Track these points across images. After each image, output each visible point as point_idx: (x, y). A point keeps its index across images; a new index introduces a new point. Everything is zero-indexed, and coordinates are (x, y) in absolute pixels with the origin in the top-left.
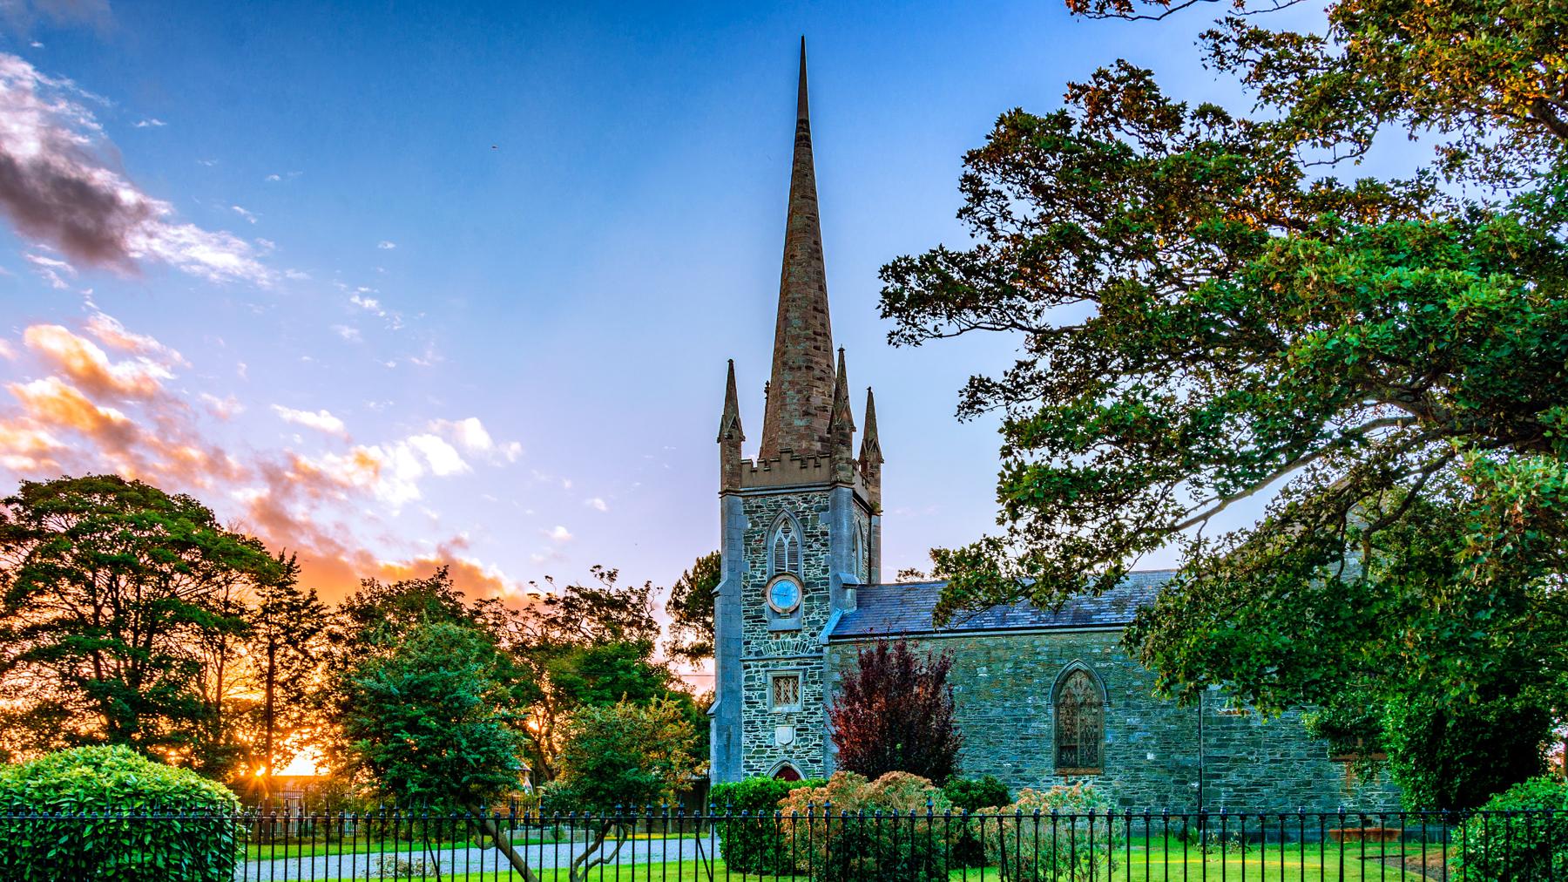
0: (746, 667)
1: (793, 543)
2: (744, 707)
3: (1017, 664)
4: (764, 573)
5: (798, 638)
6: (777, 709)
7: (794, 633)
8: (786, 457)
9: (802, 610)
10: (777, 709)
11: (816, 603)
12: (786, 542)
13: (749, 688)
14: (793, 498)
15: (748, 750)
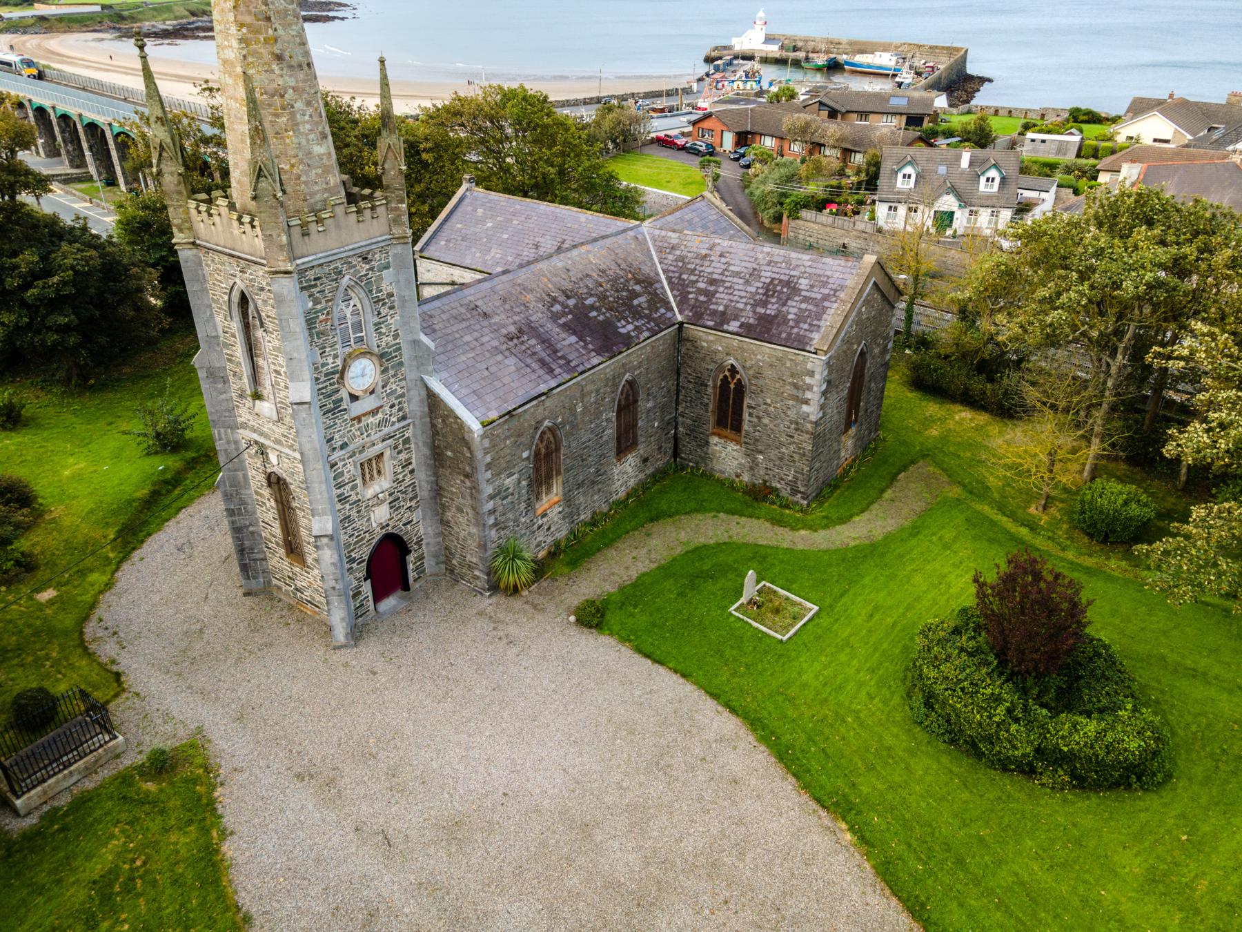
1: (356, 313)
2: (339, 506)
5: (380, 415)
6: (370, 492)
7: (374, 412)
9: (381, 384)
10: (370, 492)
12: (348, 312)
13: (339, 486)
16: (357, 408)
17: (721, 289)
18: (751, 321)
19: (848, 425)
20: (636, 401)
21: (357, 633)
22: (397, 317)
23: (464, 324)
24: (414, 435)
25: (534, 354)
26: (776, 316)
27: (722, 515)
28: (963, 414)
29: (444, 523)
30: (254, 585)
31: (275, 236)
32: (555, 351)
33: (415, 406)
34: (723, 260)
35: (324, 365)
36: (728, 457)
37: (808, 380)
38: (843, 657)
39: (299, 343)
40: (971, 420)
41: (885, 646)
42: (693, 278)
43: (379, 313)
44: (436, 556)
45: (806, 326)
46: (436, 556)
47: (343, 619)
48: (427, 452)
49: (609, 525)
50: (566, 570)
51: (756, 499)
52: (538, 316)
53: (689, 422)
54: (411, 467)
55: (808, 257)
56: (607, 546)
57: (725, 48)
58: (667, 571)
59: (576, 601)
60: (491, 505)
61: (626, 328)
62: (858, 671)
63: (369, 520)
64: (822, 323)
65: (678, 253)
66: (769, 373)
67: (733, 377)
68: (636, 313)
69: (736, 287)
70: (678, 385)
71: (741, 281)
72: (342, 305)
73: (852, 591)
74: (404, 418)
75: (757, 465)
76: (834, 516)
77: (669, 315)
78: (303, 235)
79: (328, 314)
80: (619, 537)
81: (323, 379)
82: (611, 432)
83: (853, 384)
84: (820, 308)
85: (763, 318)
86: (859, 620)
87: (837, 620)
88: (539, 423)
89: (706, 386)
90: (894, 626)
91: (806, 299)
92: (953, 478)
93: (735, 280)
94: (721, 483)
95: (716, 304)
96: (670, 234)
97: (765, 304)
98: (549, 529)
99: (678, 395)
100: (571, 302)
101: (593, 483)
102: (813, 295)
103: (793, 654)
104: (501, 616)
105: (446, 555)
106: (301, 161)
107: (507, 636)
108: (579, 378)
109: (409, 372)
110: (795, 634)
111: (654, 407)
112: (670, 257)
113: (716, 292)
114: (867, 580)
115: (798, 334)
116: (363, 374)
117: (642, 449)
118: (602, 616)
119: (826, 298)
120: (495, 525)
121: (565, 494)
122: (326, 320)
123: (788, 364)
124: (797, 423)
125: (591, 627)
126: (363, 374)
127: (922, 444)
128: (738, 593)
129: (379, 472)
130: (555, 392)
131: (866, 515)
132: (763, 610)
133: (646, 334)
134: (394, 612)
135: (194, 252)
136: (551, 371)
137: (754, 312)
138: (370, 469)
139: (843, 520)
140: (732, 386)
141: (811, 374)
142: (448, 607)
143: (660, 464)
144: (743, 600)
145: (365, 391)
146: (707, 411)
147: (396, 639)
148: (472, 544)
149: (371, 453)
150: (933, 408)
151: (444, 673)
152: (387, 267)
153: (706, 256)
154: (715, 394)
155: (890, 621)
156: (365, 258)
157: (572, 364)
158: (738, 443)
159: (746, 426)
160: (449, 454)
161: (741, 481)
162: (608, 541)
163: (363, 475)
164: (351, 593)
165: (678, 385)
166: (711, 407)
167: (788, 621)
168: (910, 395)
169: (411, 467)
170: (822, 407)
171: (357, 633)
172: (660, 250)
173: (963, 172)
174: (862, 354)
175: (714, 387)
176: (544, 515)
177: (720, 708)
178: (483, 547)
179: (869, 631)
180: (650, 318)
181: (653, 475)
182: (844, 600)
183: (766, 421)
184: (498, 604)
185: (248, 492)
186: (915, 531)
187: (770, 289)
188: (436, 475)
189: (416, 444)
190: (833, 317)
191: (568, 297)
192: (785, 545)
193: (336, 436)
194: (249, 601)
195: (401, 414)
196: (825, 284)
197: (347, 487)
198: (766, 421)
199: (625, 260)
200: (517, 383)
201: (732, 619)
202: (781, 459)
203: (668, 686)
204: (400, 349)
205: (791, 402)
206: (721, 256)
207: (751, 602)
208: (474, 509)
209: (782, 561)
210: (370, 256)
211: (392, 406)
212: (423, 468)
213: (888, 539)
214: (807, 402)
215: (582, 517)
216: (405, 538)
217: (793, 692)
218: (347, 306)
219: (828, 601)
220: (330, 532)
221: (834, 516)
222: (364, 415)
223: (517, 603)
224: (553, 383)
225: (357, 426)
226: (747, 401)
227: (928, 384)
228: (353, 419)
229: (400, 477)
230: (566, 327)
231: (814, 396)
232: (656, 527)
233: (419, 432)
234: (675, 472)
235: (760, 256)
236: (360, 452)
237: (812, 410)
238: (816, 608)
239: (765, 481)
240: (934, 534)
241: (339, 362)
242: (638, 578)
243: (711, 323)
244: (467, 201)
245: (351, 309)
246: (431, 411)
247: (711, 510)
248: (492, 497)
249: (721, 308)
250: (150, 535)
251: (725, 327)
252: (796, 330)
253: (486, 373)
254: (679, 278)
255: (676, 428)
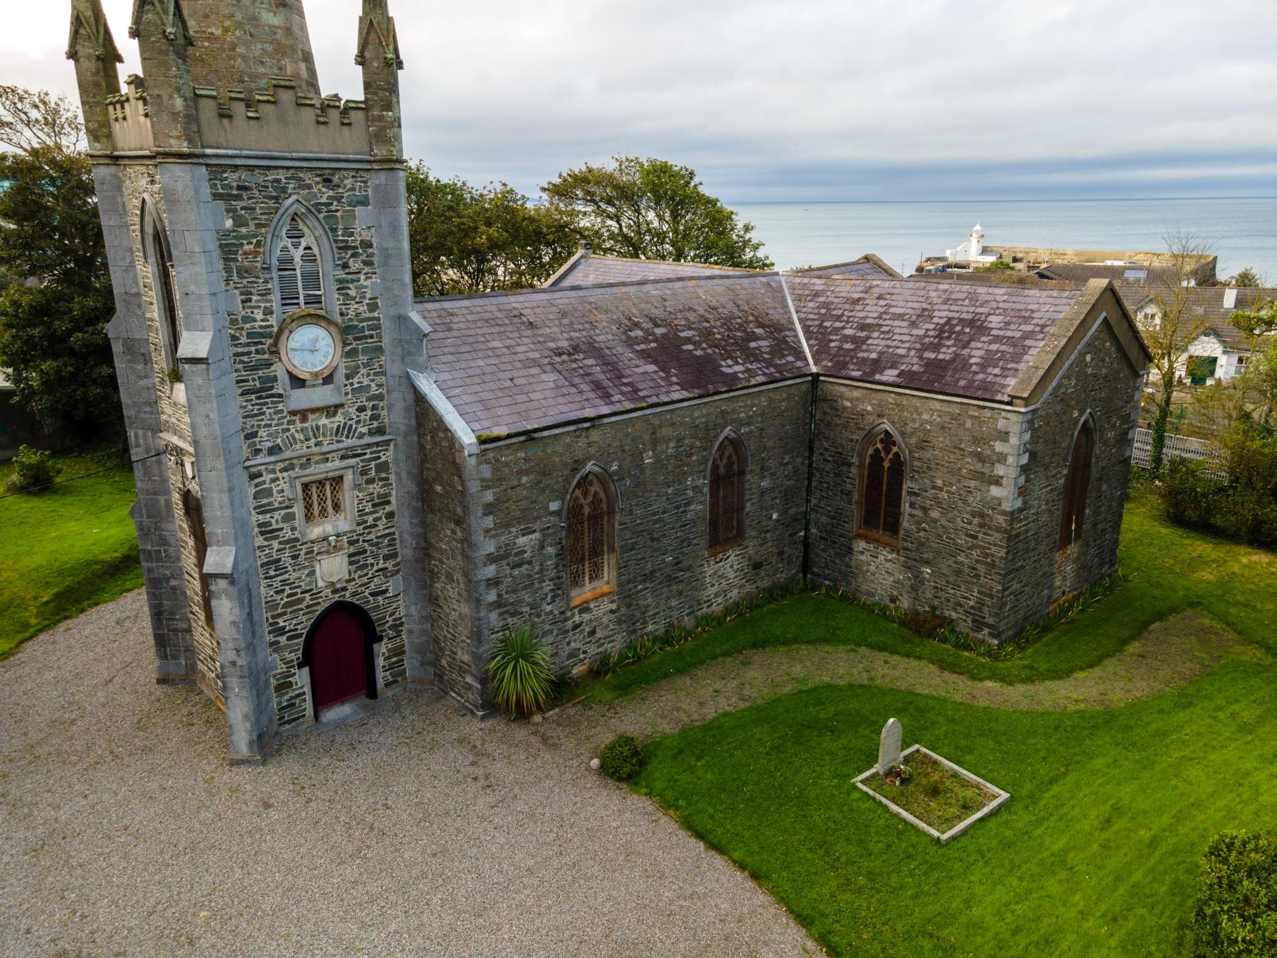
0: (253, 477)
1: (309, 257)
2: (260, 541)
3: (679, 440)
4: (268, 312)
5: (339, 418)
6: (316, 531)
7: (331, 410)
8: (286, 97)
9: (342, 372)
10: (316, 531)
11: (363, 359)
12: (297, 255)
13: (262, 510)
14: (308, 178)
15: (272, 605)
16: (301, 399)
17: (876, 334)
18: (915, 368)
19: (1065, 541)
20: (742, 473)
21: (268, 744)
22: (376, 279)
23: (497, 329)
24: (396, 461)
25: (588, 374)
26: (952, 361)
27: (863, 650)
28: (1255, 558)
29: (433, 600)
30: (177, 668)
31: (165, 98)
32: (620, 377)
33: (396, 417)
34: (882, 302)
35: (247, 319)
36: (879, 569)
37: (999, 446)
38: (1053, 886)
39: (197, 269)
40: (1269, 564)
41: (1137, 877)
42: (838, 324)
43: (345, 266)
44: (420, 651)
45: (997, 371)
46: (420, 651)
47: (246, 716)
48: (413, 488)
49: (690, 644)
50: (609, 696)
51: (918, 633)
52: (606, 337)
53: (824, 519)
54: (388, 509)
55: (1004, 291)
56: (679, 672)
57: (939, 259)
58: (761, 714)
59: (608, 738)
60: (491, 570)
61: (730, 367)
62: (1083, 915)
63: (312, 573)
64: (1022, 366)
65: (822, 299)
66: (940, 440)
67: (888, 451)
68: (752, 356)
69: (897, 330)
70: (810, 465)
71: (905, 324)
72: (288, 243)
73: (1071, 778)
74: (380, 431)
75: (922, 582)
76: (1043, 667)
77: (799, 364)
78: (222, 116)
79: (258, 244)
80: (702, 662)
81: (243, 340)
82: (699, 507)
83: (1071, 479)
84: (1019, 348)
85: (930, 364)
86: (1086, 825)
87: (1041, 821)
88: (578, 463)
89: (849, 465)
90: (1153, 843)
91: (997, 339)
92: (1245, 636)
93: (896, 323)
94: (869, 609)
95: (867, 351)
96: (814, 281)
97: (936, 348)
98: (592, 633)
99: (810, 480)
100: (659, 331)
101: (670, 579)
102: (1009, 334)
103: (958, 867)
104: (489, 747)
105: (433, 650)
106: (239, 25)
107: (487, 777)
108: (648, 412)
109: (392, 365)
110: (964, 832)
111: (772, 490)
112: (811, 305)
113: (868, 338)
114: (1098, 763)
115: (984, 381)
116: (311, 349)
117: (751, 547)
118: (641, 764)
119: (1028, 335)
120: (498, 604)
121: (620, 585)
122: (256, 254)
123: (969, 424)
124: (982, 515)
125: (620, 779)
126: (311, 349)
127: (1188, 589)
128: (871, 758)
129: (337, 507)
130: (605, 421)
131: (1097, 671)
132: (911, 787)
133: (761, 379)
134: (342, 724)
135: (113, 169)
136: (608, 396)
137: (921, 358)
138: (320, 495)
139: (1057, 675)
140: (886, 464)
141: (1004, 436)
142: (419, 726)
143: (781, 577)
144: (877, 768)
145: (316, 375)
146: (850, 503)
147: (325, 761)
148: (464, 632)
149: (318, 470)
150: (1202, 548)
151: (369, 818)
152: (364, 202)
153: (859, 299)
154: (861, 476)
155: (1144, 834)
156: (329, 181)
157: (641, 394)
158: (894, 549)
159: (905, 524)
160: (439, 488)
161: (897, 608)
162: (685, 666)
163: (308, 507)
164: (273, 682)
165: (810, 465)
166: (856, 496)
167: (954, 810)
168: (1164, 531)
169: (388, 509)
170: (1022, 492)
171: (268, 744)
172: (798, 299)
173: (1228, 311)
174: (1085, 429)
175: (861, 466)
176: (584, 609)
177: (810, 944)
178: (477, 636)
179: (1105, 846)
180: (769, 364)
181: (770, 591)
182: (1055, 789)
183: (935, 514)
184: (492, 731)
185: (170, 527)
186: (1184, 702)
187: (944, 331)
188: (424, 524)
189: (398, 474)
190: (1038, 356)
191: (657, 326)
192: (958, 698)
193: (263, 433)
194: (159, 691)
195: (375, 424)
196: (1027, 320)
197: (277, 515)
198: (935, 514)
199: (748, 303)
200: (549, 401)
201: (855, 795)
202: (958, 573)
203: (723, 889)
204: (378, 327)
205: (973, 484)
206: (879, 298)
207: (892, 772)
208: (466, 574)
209: (951, 720)
210: (336, 179)
211: (361, 409)
212: (406, 513)
213: (1135, 708)
214: (997, 481)
215: (650, 628)
216: (373, 615)
217: (951, 934)
218: (296, 246)
219: (1028, 787)
220: (228, 570)
221: (1043, 667)
222: (314, 410)
223: (520, 733)
224: (606, 410)
225: (299, 425)
226: (907, 485)
227: (1192, 510)
228: (293, 413)
229: (370, 519)
230: (646, 355)
231: (1008, 471)
232: (758, 656)
233: (402, 457)
234: (804, 590)
235: (933, 294)
236: (303, 466)
237: (1005, 494)
238: (1005, 795)
239: (933, 608)
240: (1220, 709)
241: (273, 321)
242: (715, 719)
243: (857, 374)
244: (580, 267)
245: (301, 251)
246: (419, 425)
247: (846, 642)
248: (492, 559)
249: (874, 356)
250: (97, 604)
251: (877, 377)
252: (981, 376)
253: (509, 383)
254: (820, 326)
255: (807, 530)
